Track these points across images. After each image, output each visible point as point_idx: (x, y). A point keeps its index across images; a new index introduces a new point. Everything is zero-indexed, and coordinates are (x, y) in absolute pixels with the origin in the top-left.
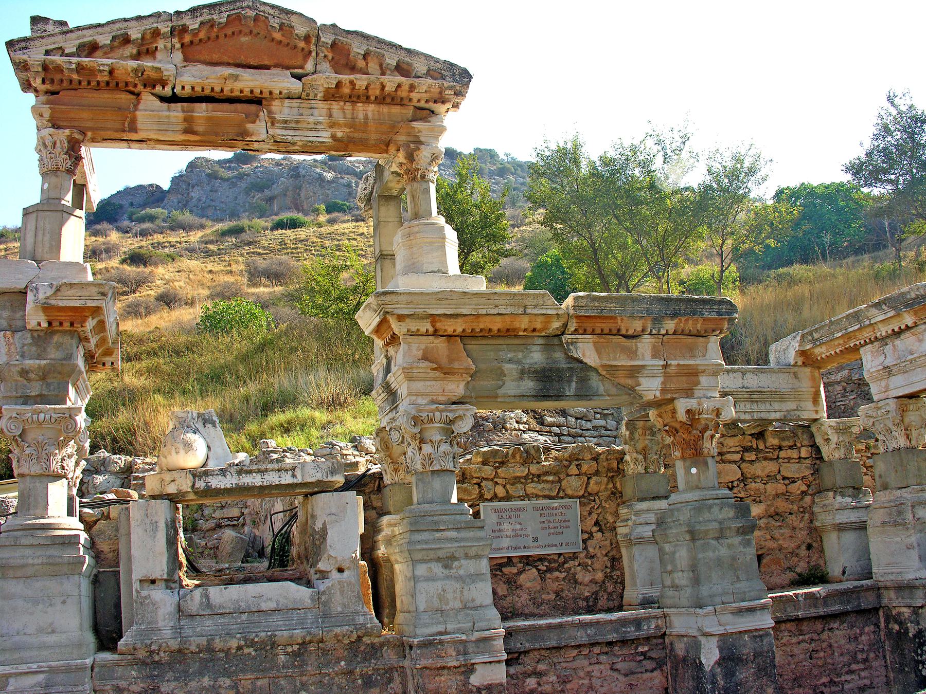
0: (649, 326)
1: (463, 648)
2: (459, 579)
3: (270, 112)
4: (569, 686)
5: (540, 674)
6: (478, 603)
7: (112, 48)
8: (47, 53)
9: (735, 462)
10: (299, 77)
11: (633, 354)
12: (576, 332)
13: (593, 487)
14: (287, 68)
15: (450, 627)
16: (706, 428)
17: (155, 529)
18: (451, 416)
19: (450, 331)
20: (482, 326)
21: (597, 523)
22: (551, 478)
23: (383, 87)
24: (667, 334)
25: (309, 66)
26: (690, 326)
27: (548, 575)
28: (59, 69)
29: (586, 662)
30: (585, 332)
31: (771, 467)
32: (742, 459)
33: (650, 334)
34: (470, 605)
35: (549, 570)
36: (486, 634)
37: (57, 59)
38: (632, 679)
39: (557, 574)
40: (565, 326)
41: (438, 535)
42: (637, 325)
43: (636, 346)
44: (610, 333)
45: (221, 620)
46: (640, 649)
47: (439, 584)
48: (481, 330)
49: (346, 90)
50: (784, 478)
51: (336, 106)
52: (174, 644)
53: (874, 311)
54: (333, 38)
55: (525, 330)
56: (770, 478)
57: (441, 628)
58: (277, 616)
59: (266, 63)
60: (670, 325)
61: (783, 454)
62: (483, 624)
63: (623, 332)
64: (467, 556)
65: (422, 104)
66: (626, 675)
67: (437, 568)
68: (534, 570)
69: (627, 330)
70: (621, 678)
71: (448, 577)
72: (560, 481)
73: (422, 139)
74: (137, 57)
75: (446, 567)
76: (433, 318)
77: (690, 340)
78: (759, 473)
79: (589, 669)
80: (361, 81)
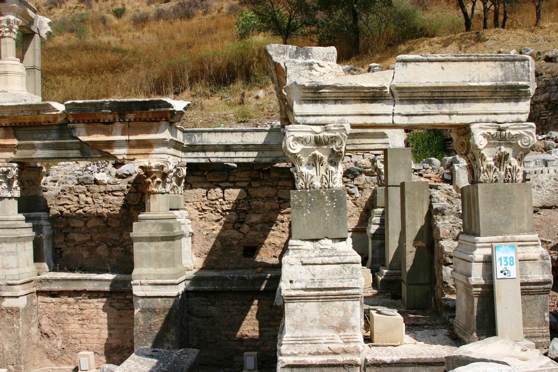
0: (117, 117)
4: (84, 312)
5: (69, 304)
6: (10, 266)
12: (73, 122)
16: (155, 178)
18: (5, 169)
19: (4, 125)
20: (20, 121)
24: (130, 121)
26: (144, 116)
27: (113, 249)
30: (79, 122)
33: (120, 121)
34: (6, 267)
35: (114, 246)
36: (10, 282)
38: (122, 313)
39: (118, 248)
40: (66, 119)
42: (111, 117)
43: (112, 128)
44: (94, 122)
46: (128, 297)
48: (20, 123)
55: (45, 122)
60: (131, 116)
62: (11, 277)
63: (102, 121)
66: (119, 310)
68: (105, 245)
69: (104, 120)
70: (115, 311)
73: (3, 13)
77: (147, 124)
79: (97, 304)
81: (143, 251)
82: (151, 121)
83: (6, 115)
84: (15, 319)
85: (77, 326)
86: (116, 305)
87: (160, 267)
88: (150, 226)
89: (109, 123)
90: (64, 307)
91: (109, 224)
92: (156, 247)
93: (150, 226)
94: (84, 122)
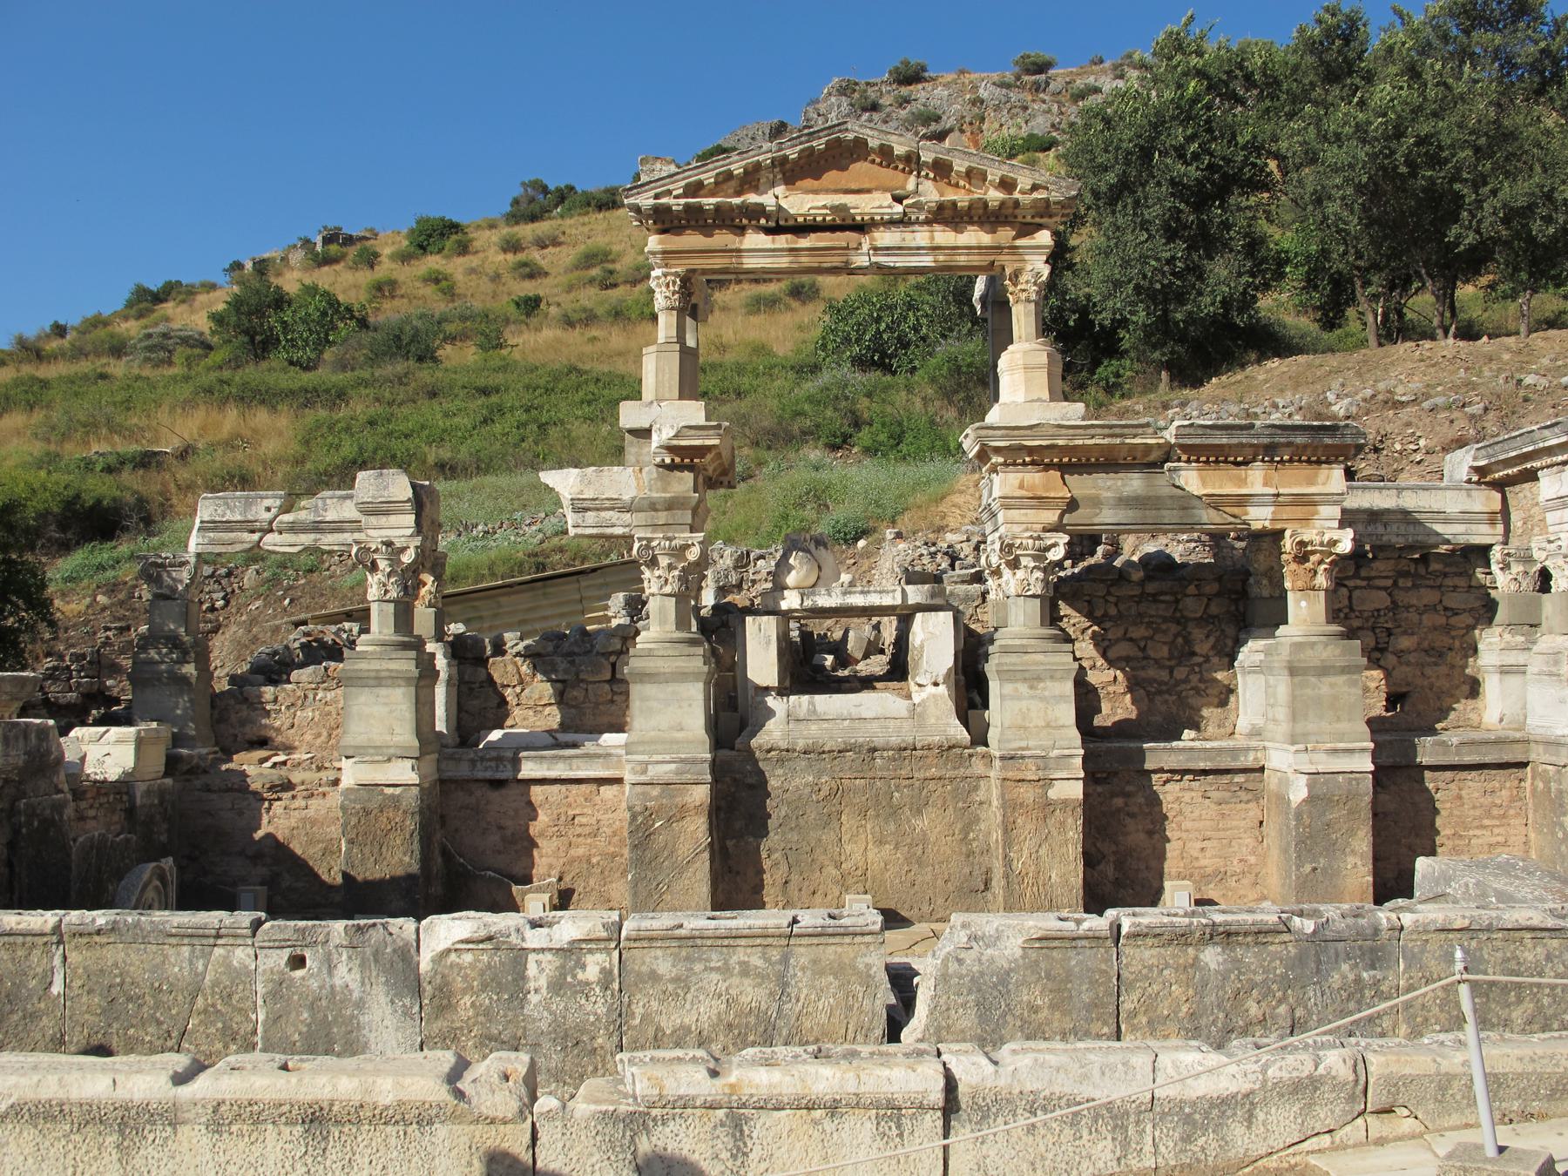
1: (1043, 761)
2: (1042, 699)
3: (872, 239)
5: (1127, 795)
7: (716, 183)
8: (657, 197)
9: (1385, 589)
10: (898, 199)
11: (1243, 482)
13: (1214, 609)
14: (885, 190)
15: (1031, 744)
17: (768, 643)
21: (1213, 647)
22: (1167, 598)
23: (985, 204)
25: (911, 186)
28: (668, 208)
29: (1177, 786)
31: (1429, 597)
32: (1395, 583)
35: (1160, 692)
36: (1067, 752)
37: (663, 200)
41: (1027, 657)
45: (825, 725)
47: (1024, 704)
49: (947, 213)
50: (1446, 609)
51: (937, 227)
52: (783, 745)
53: (1546, 432)
54: (933, 155)
56: (1429, 608)
57: (1023, 744)
58: (875, 724)
59: (866, 186)
61: (1448, 582)
62: (1065, 743)
64: (1052, 677)
65: (1029, 219)
67: (1023, 688)
70: (1213, 806)
71: (1032, 697)
72: (1177, 601)
74: (738, 194)
75: (1031, 687)
76: (1031, 450)
78: (1414, 602)
80: (961, 198)
81: (1309, 691)
82: (1319, 462)
83: (1061, 443)
84: (1070, 820)
85: (1142, 836)
86: (1215, 795)
87: (1339, 719)
88: (1320, 647)
89: (1245, 463)
90: (1119, 802)
91: (1151, 653)
92: (1332, 685)
93: (1320, 647)
94: (1197, 461)
